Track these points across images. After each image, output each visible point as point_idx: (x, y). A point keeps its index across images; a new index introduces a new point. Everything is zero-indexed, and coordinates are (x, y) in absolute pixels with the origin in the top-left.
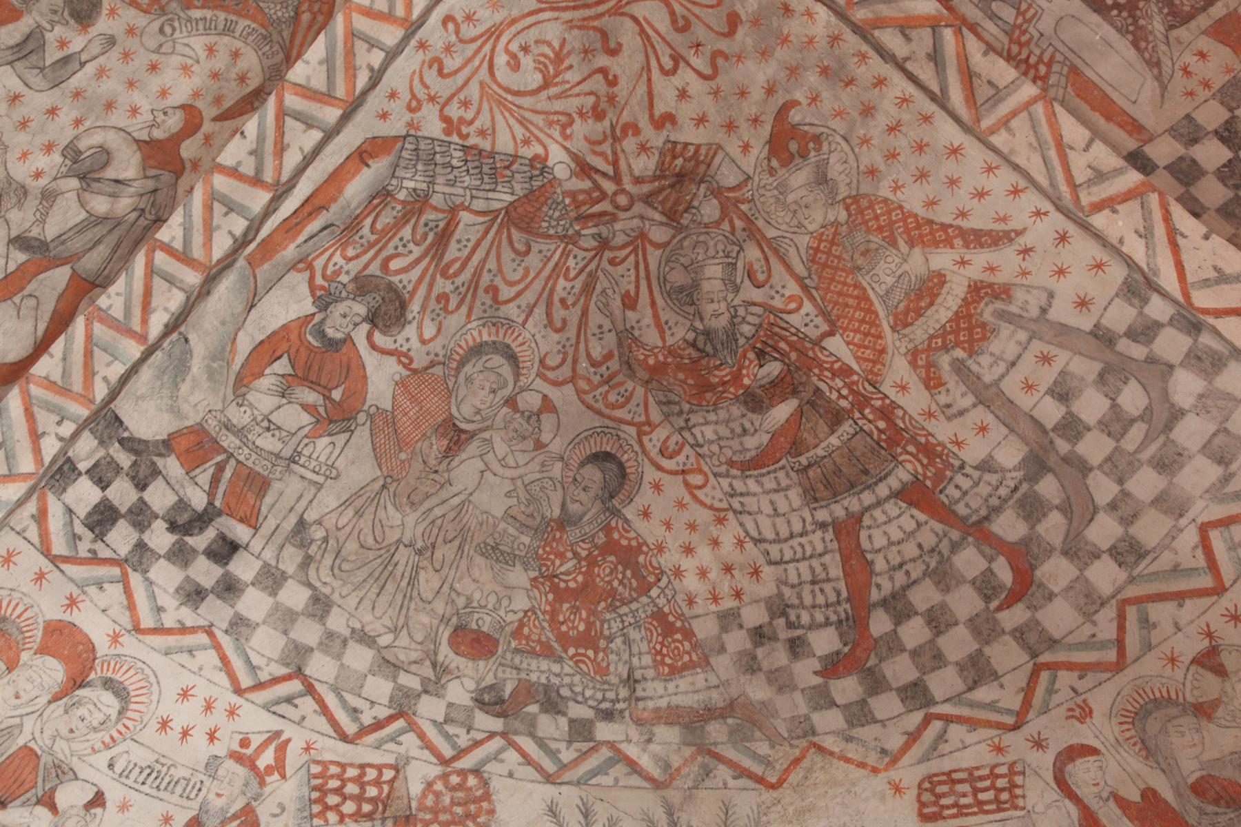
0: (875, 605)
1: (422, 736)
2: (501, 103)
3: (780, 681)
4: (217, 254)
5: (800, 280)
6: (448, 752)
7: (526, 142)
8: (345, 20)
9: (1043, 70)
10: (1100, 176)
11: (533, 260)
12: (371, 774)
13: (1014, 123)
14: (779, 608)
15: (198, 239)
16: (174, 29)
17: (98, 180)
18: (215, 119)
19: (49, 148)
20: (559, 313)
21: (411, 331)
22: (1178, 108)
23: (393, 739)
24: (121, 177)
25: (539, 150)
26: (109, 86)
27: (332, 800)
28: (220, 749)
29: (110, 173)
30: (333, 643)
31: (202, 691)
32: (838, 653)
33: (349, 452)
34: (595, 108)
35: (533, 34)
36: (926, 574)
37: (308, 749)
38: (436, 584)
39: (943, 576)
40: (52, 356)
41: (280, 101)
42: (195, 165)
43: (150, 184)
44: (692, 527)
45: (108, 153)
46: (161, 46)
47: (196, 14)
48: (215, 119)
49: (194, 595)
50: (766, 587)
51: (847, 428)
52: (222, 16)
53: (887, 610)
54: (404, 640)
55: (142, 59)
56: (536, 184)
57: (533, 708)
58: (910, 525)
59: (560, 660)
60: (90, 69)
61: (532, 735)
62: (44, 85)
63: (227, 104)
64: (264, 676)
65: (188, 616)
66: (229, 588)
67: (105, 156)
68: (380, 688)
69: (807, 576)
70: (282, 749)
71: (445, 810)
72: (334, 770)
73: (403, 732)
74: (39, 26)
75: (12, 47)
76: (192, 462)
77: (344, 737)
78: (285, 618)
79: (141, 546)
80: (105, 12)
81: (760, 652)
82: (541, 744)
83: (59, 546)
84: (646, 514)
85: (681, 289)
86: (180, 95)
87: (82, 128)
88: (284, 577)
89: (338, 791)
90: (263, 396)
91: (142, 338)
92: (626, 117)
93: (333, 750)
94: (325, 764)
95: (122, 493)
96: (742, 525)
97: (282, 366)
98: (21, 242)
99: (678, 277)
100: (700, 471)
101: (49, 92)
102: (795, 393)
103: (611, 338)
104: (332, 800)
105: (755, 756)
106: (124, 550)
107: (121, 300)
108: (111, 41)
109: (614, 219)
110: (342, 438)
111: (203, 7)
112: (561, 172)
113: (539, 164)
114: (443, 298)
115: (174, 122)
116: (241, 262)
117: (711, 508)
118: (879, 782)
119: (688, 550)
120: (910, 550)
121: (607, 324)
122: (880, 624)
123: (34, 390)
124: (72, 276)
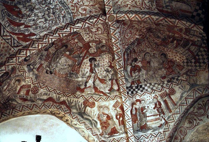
0: (196, 56)
1: (165, 88)
2: (129, 39)
3: (192, 66)
4: (123, 75)
5: (168, 32)
6: (168, 88)
7: (134, 39)
9: (177, 11)
10: (190, 25)
11: (143, 45)
12: (164, 93)
13: (178, 24)
14: (187, 59)
15: (121, 75)
18: (112, 62)
20: (149, 47)
21: (139, 59)
22: (193, 8)
23: (164, 89)
25: (136, 38)
27: (163, 96)
28: (153, 98)
30: (154, 86)
31: (148, 96)
32: (195, 61)
33: (143, 72)
34: (137, 31)
35: (127, 33)
36: (199, 51)
37: (158, 94)
38: (157, 75)
39: (201, 51)
41: (117, 61)
44: (174, 55)
47: (102, 54)
48: (112, 62)
49: (142, 91)
50: (185, 58)
51: (182, 41)
53: (197, 56)
54: (159, 82)
55: (102, 60)
56: (138, 40)
57: (172, 80)
58: (194, 47)
59: (171, 75)
61: (174, 82)
64: (151, 92)
65: (143, 93)
66: (144, 88)
68: (160, 86)
69: (188, 55)
70: (157, 95)
71: (171, 92)
72: (161, 94)
73: (164, 89)
76: (134, 84)
77: (160, 92)
78: (149, 87)
79: (136, 91)
81: (188, 64)
82: (175, 82)
83: (132, 96)
84: (170, 56)
85: (157, 37)
86: (108, 61)
88: (146, 84)
89: (163, 96)
90: (134, 75)
91: (125, 84)
92: (140, 29)
93: (160, 93)
94: (160, 94)
95: (132, 90)
96: (179, 53)
97: (133, 72)
99: (156, 36)
100: (172, 50)
102: (175, 40)
103: (155, 44)
104: (163, 96)
105: (193, 74)
106: (135, 93)
109: (146, 36)
110: (141, 71)
112: (138, 37)
113: (137, 39)
114: (139, 55)
115: (109, 63)
116: (124, 70)
117: (175, 53)
118: (205, 72)
119: (176, 58)
120: (196, 50)
121: (153, 44)
122: (197, 57)
123: (123, 93)
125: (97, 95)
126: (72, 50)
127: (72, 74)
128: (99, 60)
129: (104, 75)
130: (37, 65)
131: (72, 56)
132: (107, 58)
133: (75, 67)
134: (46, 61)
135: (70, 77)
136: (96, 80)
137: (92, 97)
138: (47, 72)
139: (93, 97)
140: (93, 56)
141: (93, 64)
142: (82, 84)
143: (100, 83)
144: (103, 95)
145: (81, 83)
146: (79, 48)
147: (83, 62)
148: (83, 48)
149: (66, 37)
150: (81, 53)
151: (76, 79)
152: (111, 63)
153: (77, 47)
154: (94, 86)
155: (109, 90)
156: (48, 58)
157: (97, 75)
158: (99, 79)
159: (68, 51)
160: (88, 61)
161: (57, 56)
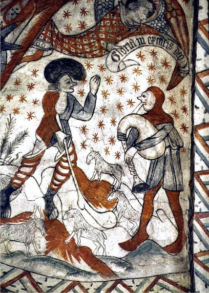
8: (203, 31)
16: (118, 56)
17: (141, 143)
18: (169, 89)
19: (112, 141)
24: (149, 136)
26: (114, 98)
29: (143, 137)
40: (196, 243)
42: (176, 115)
43: (163, 133)
45: (136, 128)
46: (119, 67)
47: (122, 43)
52: (134, 38)
55: (116, 78)
60: (99, 95)
62: (89, 116)
63: (168, 80)
67: (135, 130)
74: (68, 93)
75: (66, 110)
80: (86, 67)
86: (144, 85)
87: (117, 124)
98: (136, 189)
101: (93, 117)
107: (202, 203)
111: (123, 39)
115: (151, 98)
123: (201, 259)
124: (166, 192)
125: (56, 263)
128: (98, 78)
129: (112, 159)
132: (144, 66)
136: (63, 182)
137: (27, 273)
139: (35, 276)
140: (71, 53)
141: (63, 96)
143: (83, 202)
144: (88, 269)
147: (14, 76)
152: (160, 98)
154: (48, 215)
155: (123, 246)
158: (81, 177)
160: (41, 74)
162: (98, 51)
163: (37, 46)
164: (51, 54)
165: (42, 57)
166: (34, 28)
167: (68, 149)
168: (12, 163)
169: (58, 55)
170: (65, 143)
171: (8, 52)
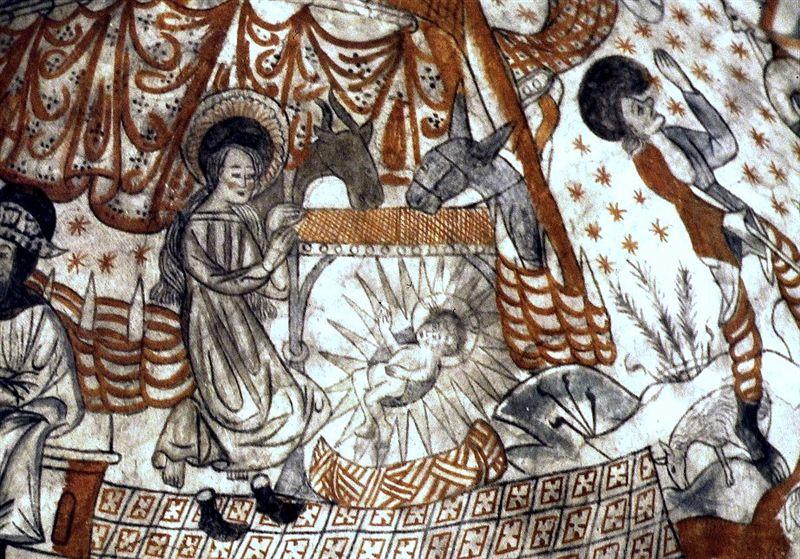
60: (699, 85)
75: (692, 164)
80: (627, 54)
87: (772, 112)
108: (660, 54)
126: (339, 126)
127: (543, 393)
130: (24, 502)
131: (394, 198)
133: (524, 303)
134: (112, 410)
135: (543, 441)
138: (214, 519)
142: (723, 462)
145: (701, 458)
146: (387, 71)
147: (557, 186)
148: (418, 37)
149: (108, 50)
150: (456, 100)
151: (626, 441)
153: (357, 60)
156: (122, 371)
157: (787, 250)
159: (311, 163)
160: (590, 138)
161: (242, 295)
162: (603, 8)
163: (529, 96)
164: (563, 87)
165: (557, 107)
166: (489, 71)
167: (767, 238)
168: (712, 355)
169: (574, 79)
170: (754, 231)
171: (503, 153)
